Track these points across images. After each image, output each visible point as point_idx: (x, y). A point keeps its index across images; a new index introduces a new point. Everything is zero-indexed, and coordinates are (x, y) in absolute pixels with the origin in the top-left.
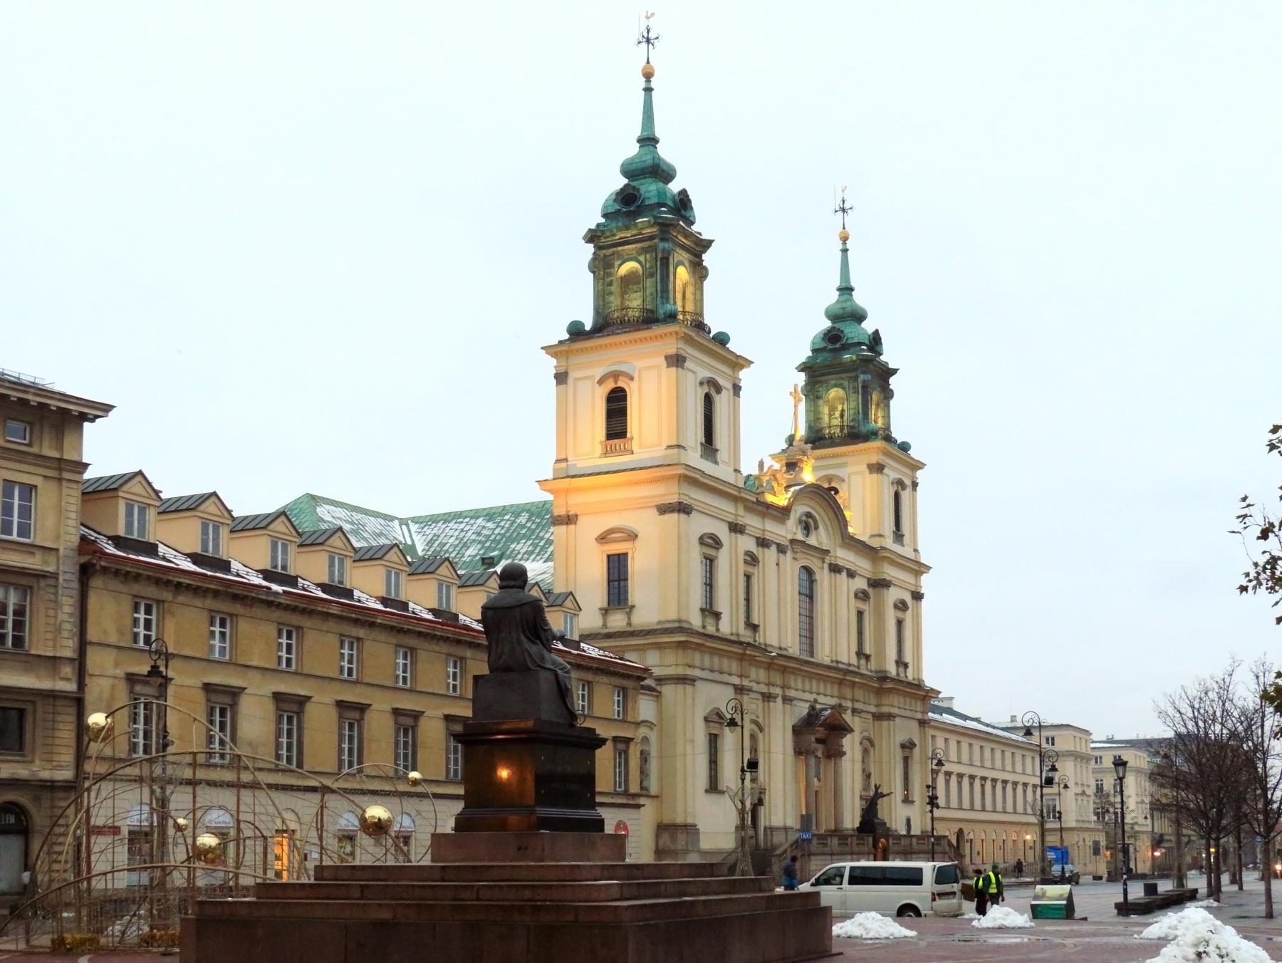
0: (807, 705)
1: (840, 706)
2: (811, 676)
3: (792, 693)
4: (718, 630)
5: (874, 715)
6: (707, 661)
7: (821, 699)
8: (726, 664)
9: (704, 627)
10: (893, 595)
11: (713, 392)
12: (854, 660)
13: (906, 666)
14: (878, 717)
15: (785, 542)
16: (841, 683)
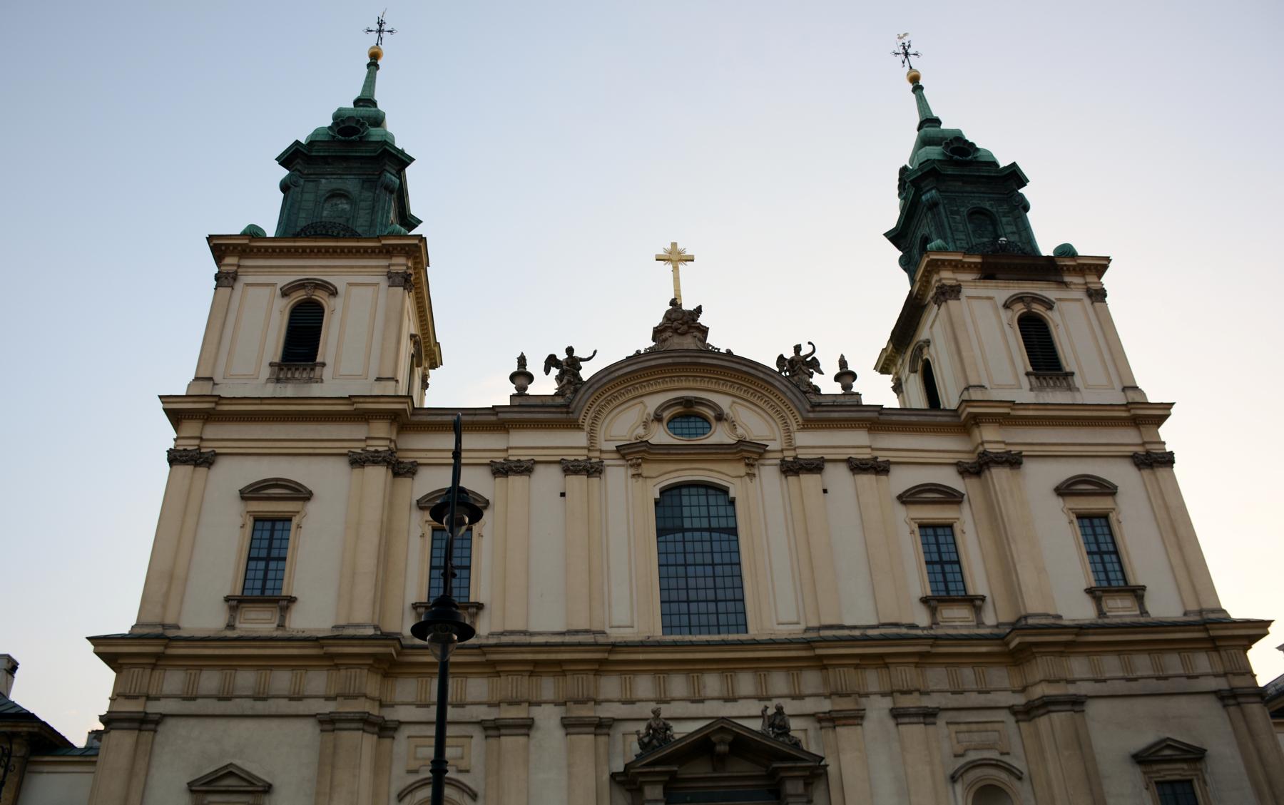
0: (642, 727)
1: (780, 710)
2: (727, 668)
3: (606, 712)
4: (281, 626)
5: (1012, 710)
6: (210, 680)
7: (667, 711)
8: (282, 680)
9: (230, 626)
10: (1041, 478)
11: (320, 296)
12: (921, 617)
13: (1138, 593)
14: (1027, 713)
15: (581, 456)
16: (821, 664)
